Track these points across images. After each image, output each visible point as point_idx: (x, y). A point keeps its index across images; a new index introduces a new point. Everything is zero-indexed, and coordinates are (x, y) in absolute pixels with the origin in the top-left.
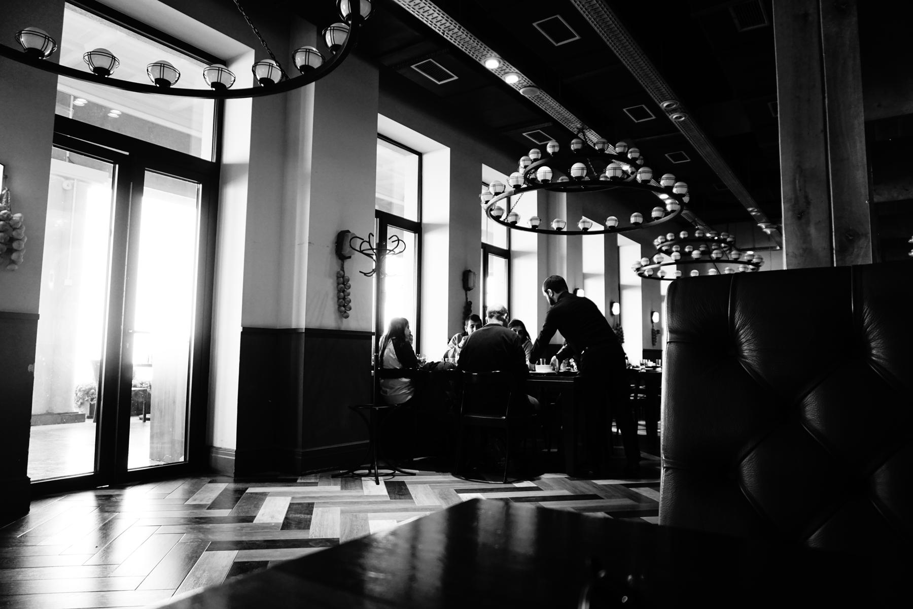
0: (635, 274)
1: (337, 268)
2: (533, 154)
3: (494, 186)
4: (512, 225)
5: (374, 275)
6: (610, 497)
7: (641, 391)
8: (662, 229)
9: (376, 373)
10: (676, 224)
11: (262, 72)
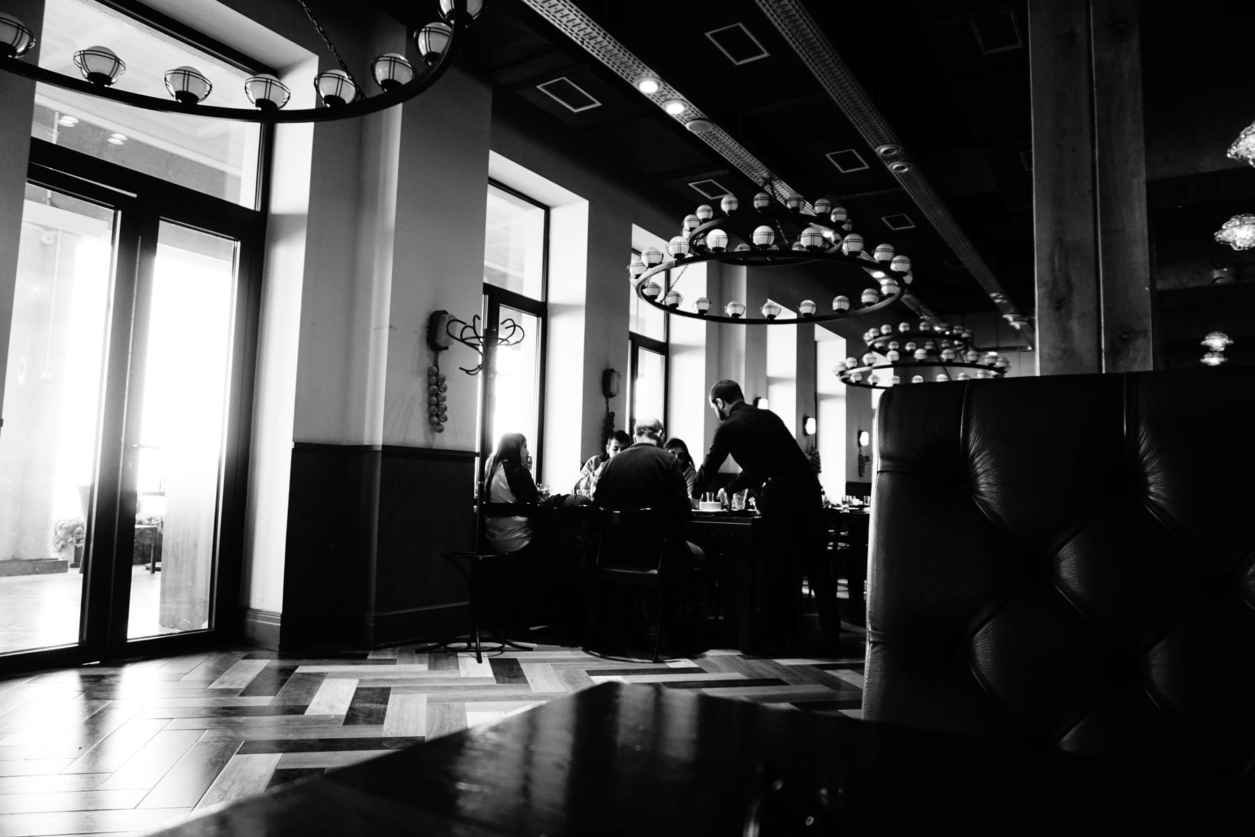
0: (838, 379)
1: (427, 362)
2: (702, 212)
3: (648, 254)
4: (672, 309)
5: (480, 373)
6: (800, 682)
7: (843, 539)
8: (876, 319)
9: (479, 508)
10: (894, 312)
11: (328, 88)
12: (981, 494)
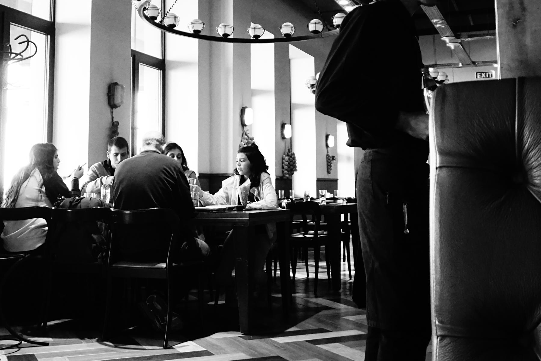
4: (171, 28)
12: (534, 185)
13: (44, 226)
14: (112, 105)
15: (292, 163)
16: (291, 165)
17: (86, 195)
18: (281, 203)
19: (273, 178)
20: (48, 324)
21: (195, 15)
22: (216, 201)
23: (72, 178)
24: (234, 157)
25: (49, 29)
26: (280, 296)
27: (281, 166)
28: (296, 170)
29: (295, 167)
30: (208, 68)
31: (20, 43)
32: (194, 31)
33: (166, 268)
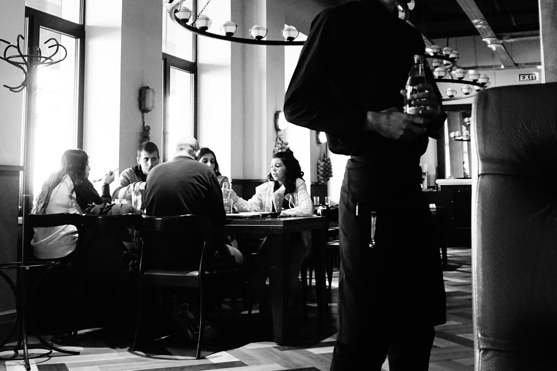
4: (203, 31)
5: (25, 90)
9: (25, 220)
13: (74, 233)
14: (143, 109)
15: (327, 168)
16: (326, 171)
17: (117, 202)
18: (316, 210)
19: (308, 184)
20: (79, 332)
21: (228, 17)
22: (250, 207)
23: (102, 183)
24: (269, 163)
25: (79, 32)
26: (316, 305)
27: (316, 172)
28: (331, 176)
29: (331, 172)
30: (241, 71)
31: (49, 47)
32: (227, 33)
33: (198, 276)
